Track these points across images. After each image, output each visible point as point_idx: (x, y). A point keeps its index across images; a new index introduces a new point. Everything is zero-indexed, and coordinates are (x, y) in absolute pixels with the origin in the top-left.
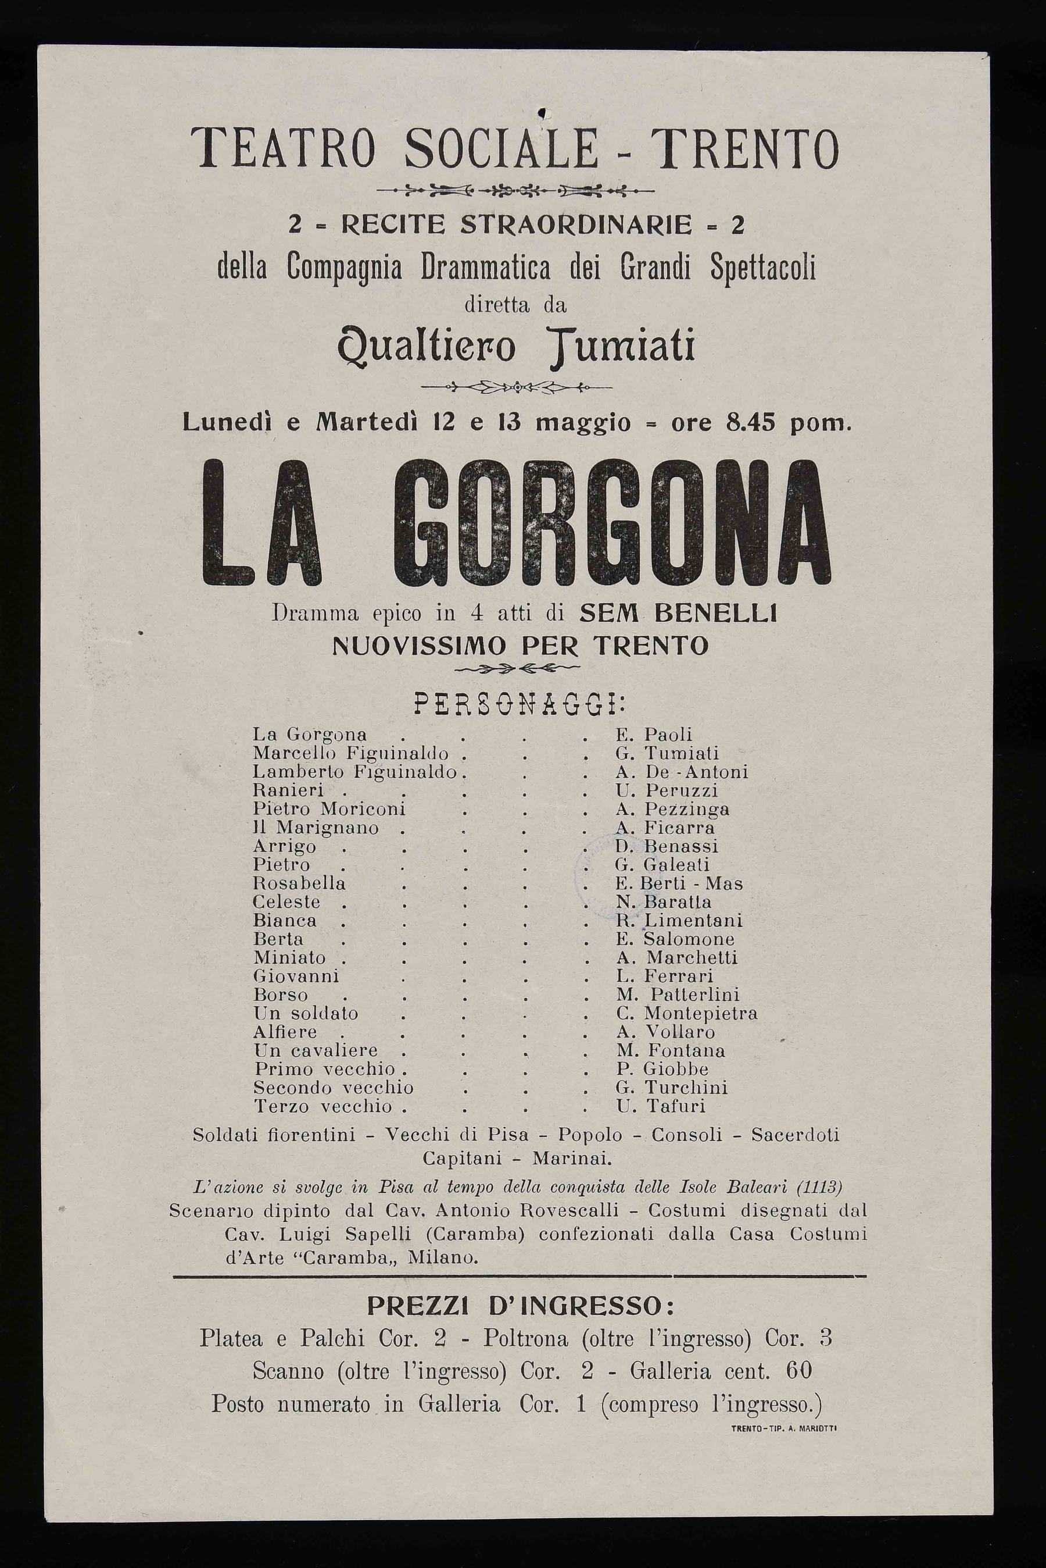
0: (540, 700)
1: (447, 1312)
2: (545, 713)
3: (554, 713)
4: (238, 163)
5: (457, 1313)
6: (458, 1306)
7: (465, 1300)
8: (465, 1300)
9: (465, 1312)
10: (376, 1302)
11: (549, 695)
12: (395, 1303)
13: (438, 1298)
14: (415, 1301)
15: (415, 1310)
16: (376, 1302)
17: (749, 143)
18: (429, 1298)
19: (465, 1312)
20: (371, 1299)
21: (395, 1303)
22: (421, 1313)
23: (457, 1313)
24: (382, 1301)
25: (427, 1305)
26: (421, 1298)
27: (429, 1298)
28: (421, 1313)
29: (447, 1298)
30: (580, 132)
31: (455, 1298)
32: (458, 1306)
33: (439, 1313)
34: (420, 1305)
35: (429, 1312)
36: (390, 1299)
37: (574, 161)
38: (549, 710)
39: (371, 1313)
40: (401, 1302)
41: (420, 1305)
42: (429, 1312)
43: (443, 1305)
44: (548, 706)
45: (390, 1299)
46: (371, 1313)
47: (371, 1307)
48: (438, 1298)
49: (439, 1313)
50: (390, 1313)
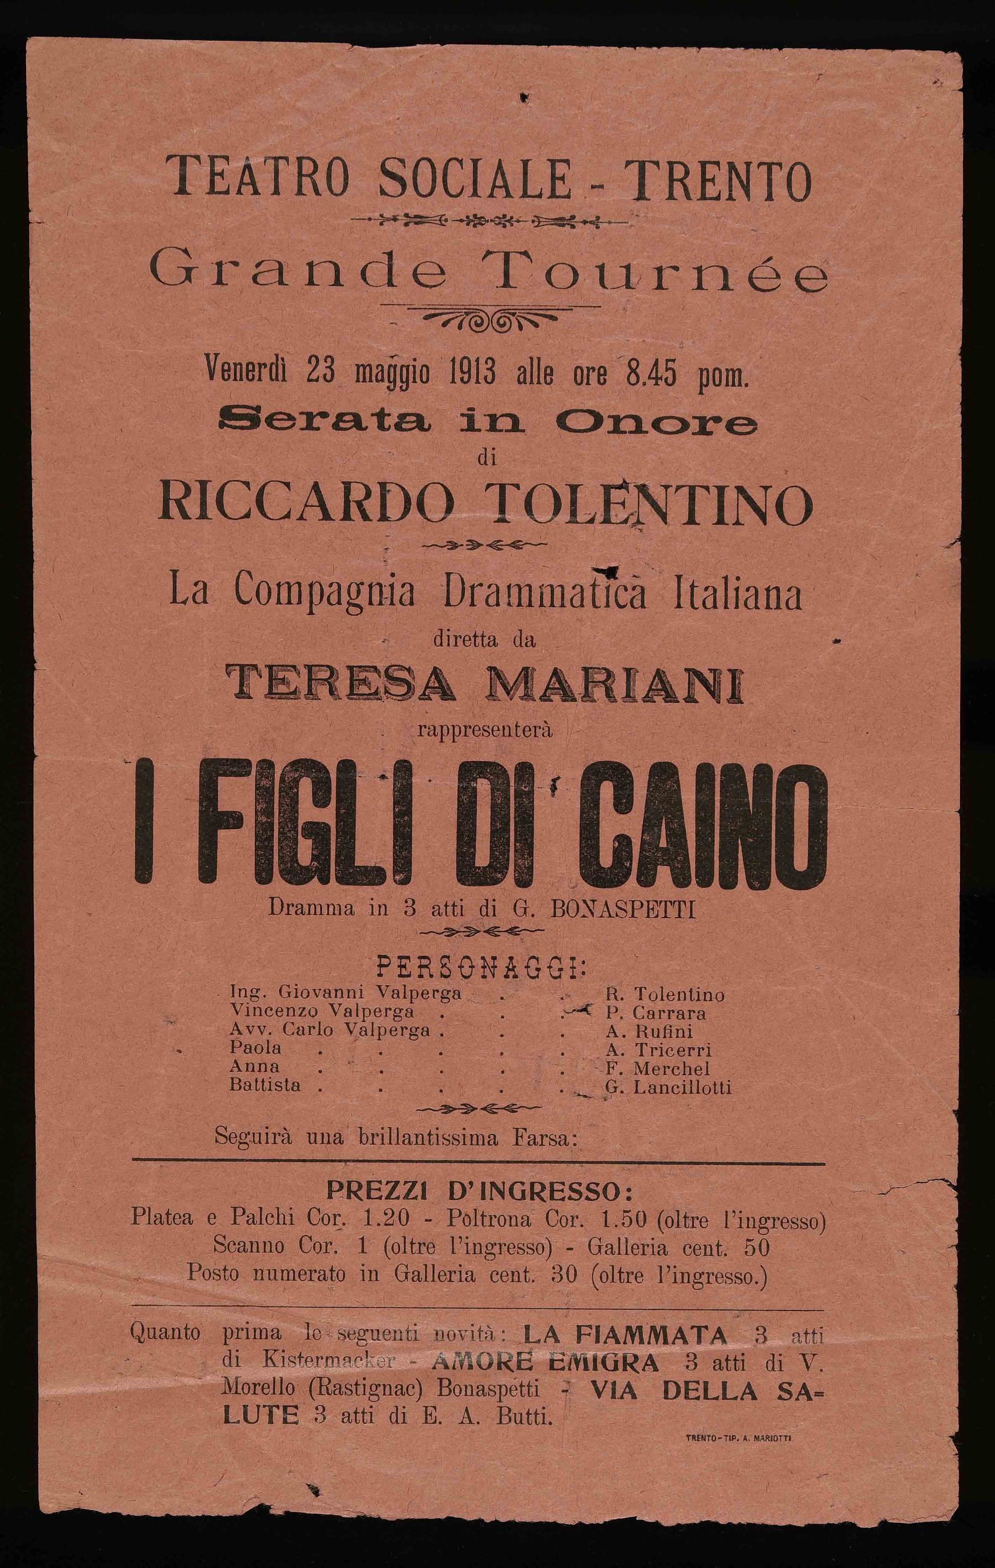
0: (502, 964)
1: (406, 1197)
2: (507, 976)
3: (515, 977)
4: (212, 191)
5: (415, 1198)
6: (418, 1190)
7: (424, 1184)
8: (424, 1184)
9: (424, 1197)
10: (336, 1186)
11: (511, 958)
13: (397, 1183)
14: (374, 1186)
15: (374, 1194)
16: (336, 1186)
17: (722, 176)
20: (330, 1183)
21: (354, 1187)
22: (380, 1198)
23: (415, 1198)
24: (341, 1187)
25: (385, 1190)
26: (380, 1182)
27: (388, 1183)
28: (380, 1198)
29: (406, 1183)
30: (553, 162)
31: (414, 1183)
32: (418, 1190)
34: (379, 1190)
35: (388, 1197)
36: (349, 1183)
37: (547, 192)
38: (511, 974)
39: (330, 1197)
40: (360, 1186)
41: (379, 1190)
42: (388, 1197)
43: (401, 1190)
44: (509, 970)
45: (349, 1183)
46: (330, 1197)
47: (330, 1192)
48: (397, 1183)
49: (398, 1198)
50: (349, 1197)
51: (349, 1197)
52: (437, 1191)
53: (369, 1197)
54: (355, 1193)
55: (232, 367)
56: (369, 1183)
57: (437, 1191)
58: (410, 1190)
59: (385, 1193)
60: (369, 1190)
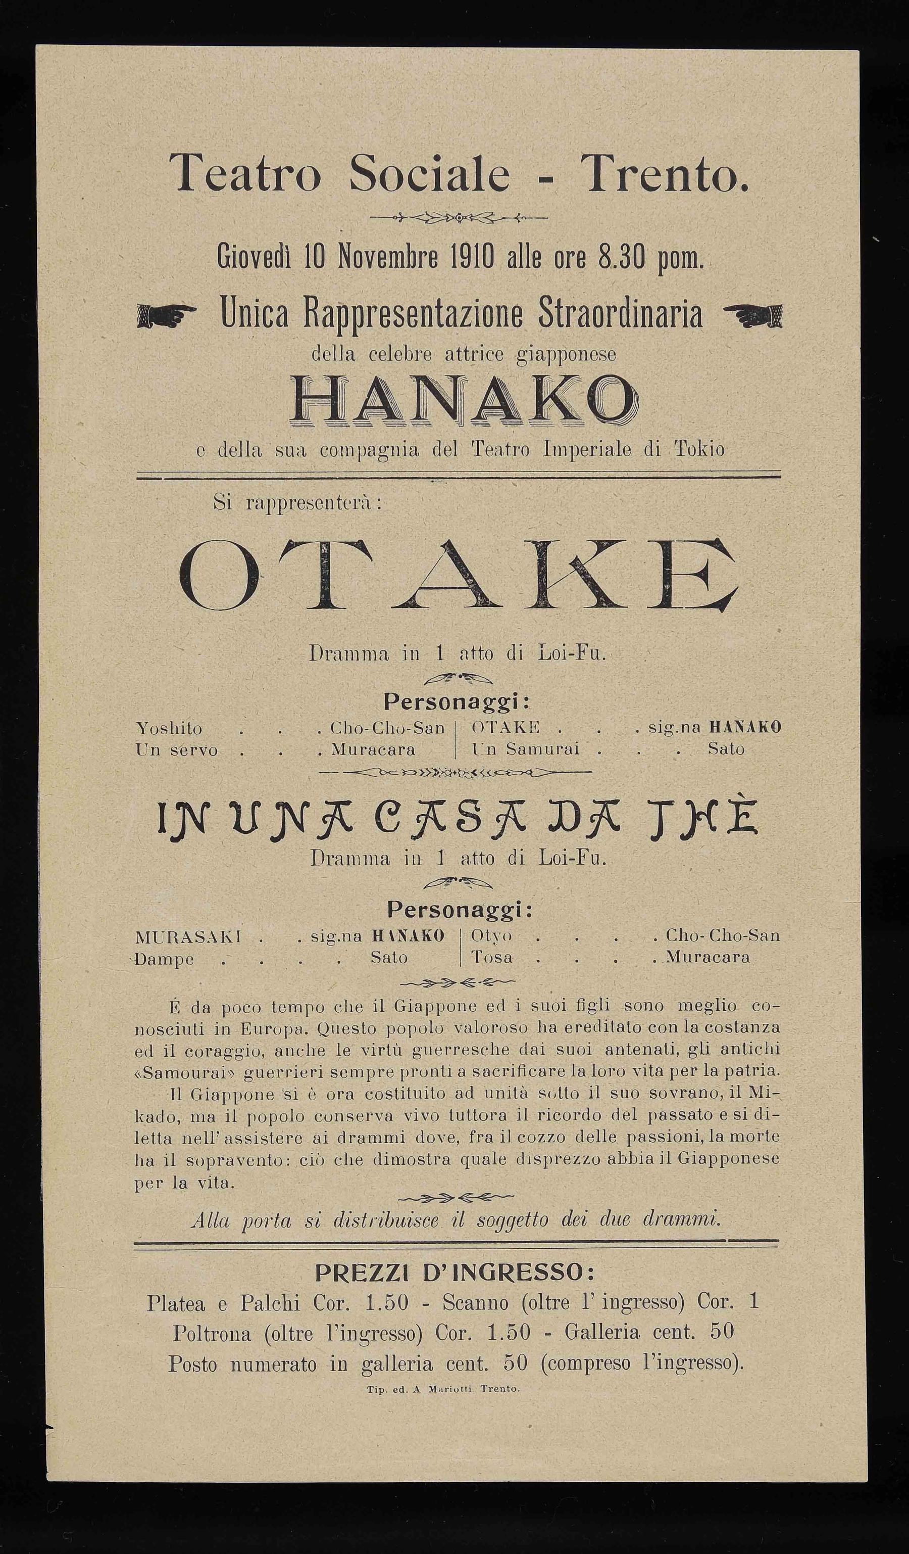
5: (398, 1280)
6: (400, 1272)
9: (406, 1279)
19: (406, 1279)
23: (398, 1280)
32: (400, 1272)
55: (388, 255)
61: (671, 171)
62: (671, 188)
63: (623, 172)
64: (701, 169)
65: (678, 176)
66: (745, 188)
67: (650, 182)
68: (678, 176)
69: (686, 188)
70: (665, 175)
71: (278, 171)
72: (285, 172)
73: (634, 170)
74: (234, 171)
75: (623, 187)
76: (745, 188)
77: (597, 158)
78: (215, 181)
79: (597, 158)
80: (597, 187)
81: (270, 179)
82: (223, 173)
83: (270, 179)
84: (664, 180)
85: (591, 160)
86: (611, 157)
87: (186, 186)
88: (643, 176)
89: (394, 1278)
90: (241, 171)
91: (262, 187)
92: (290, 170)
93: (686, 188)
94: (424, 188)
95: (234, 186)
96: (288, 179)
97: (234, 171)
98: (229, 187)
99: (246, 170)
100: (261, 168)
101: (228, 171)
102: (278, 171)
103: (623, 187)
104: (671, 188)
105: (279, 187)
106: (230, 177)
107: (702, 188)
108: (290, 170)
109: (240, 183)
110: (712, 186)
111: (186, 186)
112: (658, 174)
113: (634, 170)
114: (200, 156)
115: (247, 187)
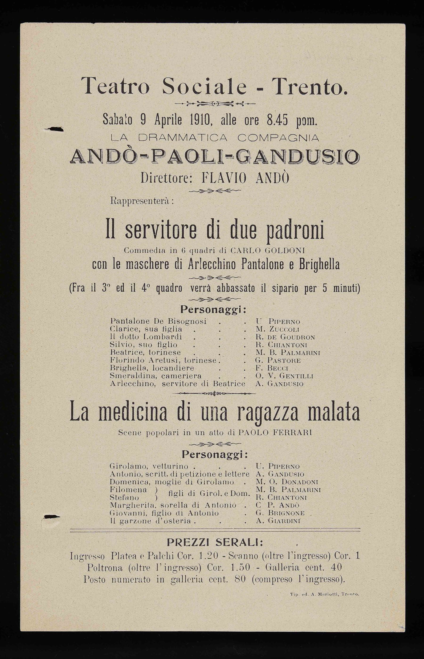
1: (200, 545)
5: (204, 545)
6: (205, 542)
7: (208, 539)
8: (208, 539)
9: (208, 545)
10: (171, 541)
12: (179, 541)
18: (193, 539)
19: (208, 545)
21: (179, 541)
25: (192, 542)
26: (189, 539)
27: (193, 539)
28: (189, 545)
31: (204, 539)
32: (205, 542)
33: (197, 545)
35: (193, 545)
36: (176, 539)
43: (198, 542)
45: (176, 539)
46: (168, 545)
49: (197, 545)
50: (176, 545)
51: (176, 545)
52: (213, 542)
53: (185, 545)
54: (179, 544)
56: (185, 539)
57: (213, 542)
58: (202, 542)
59: (191, 544)
60: (185, 542)
61: (312, 86)
62: (312, 93)
63: (291, 86)
64: (326, 84)
65: (316, 88)
66: (346, 93)
67: (303, 90)
68: (316, 88)
69: (319, 93)
70: (310, 87)
71: (130, 85)
72: (133, 86)
73: (296, 85)
74: (110, 85)
75: (291, 93)
76: (346, 93)
77: (279, 80)
78: (102, 89)
79: (279, 80)
80: (279, 93)
81: (126, 88)
82: (105, 86)
83: (126, 88)
84: (309, 90)
85: (277, 80)
86: (285, 79)
87: (88, 92)
88: (300, 87)
89: (202, 544)
90: (113, 85)
91: (123, 92)
92: (136, 84)
93: (319, 93)
94: (199, 93)
95: (110, 92)
96: (135, 89)
97: (110, 85)
98: (108, 92)
99: (116, 84)
100: (123, 83)
101: (108, 85)
102: (130, 85)
103: (291, 93)
104: (312, 93)
105: (130, 92)
106: (108, 87)
107: (327, 93)
108: (136, 84)
109: (113, 90)
110: (331, 92)
111: (88, 92)
112: (307, 87)
113: (296, 85)
114: (95, 78)
115: (116, 92)
